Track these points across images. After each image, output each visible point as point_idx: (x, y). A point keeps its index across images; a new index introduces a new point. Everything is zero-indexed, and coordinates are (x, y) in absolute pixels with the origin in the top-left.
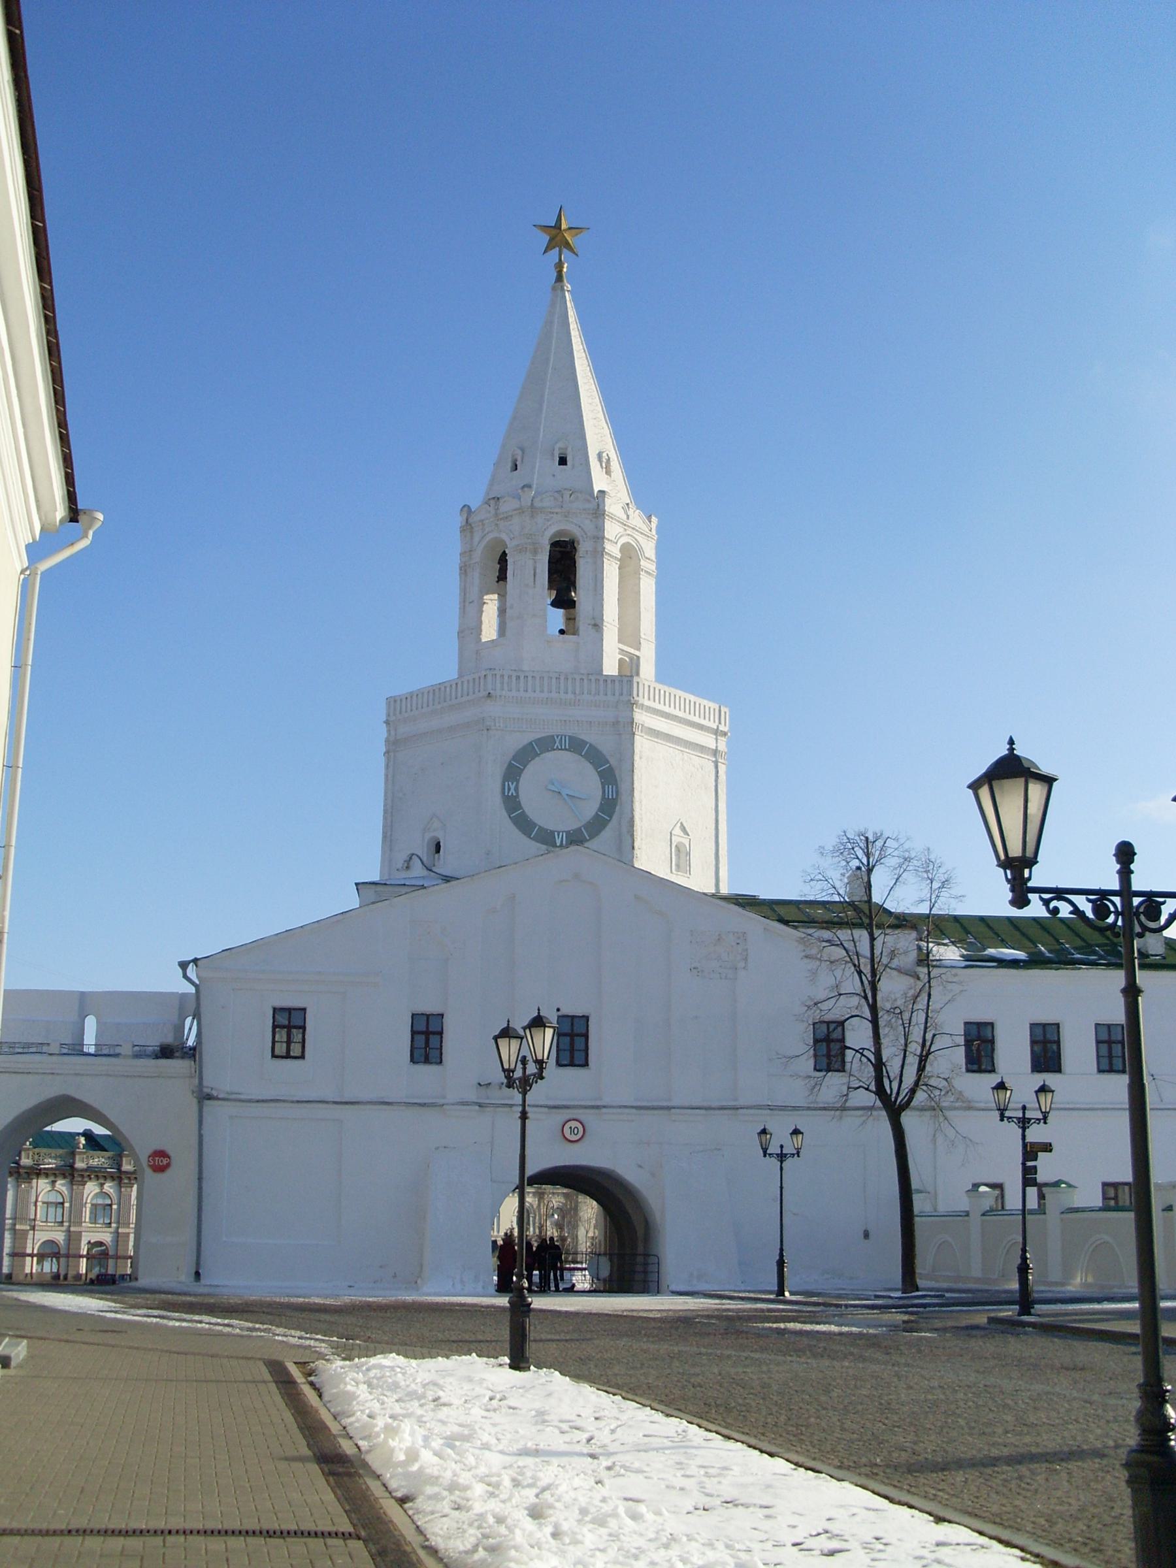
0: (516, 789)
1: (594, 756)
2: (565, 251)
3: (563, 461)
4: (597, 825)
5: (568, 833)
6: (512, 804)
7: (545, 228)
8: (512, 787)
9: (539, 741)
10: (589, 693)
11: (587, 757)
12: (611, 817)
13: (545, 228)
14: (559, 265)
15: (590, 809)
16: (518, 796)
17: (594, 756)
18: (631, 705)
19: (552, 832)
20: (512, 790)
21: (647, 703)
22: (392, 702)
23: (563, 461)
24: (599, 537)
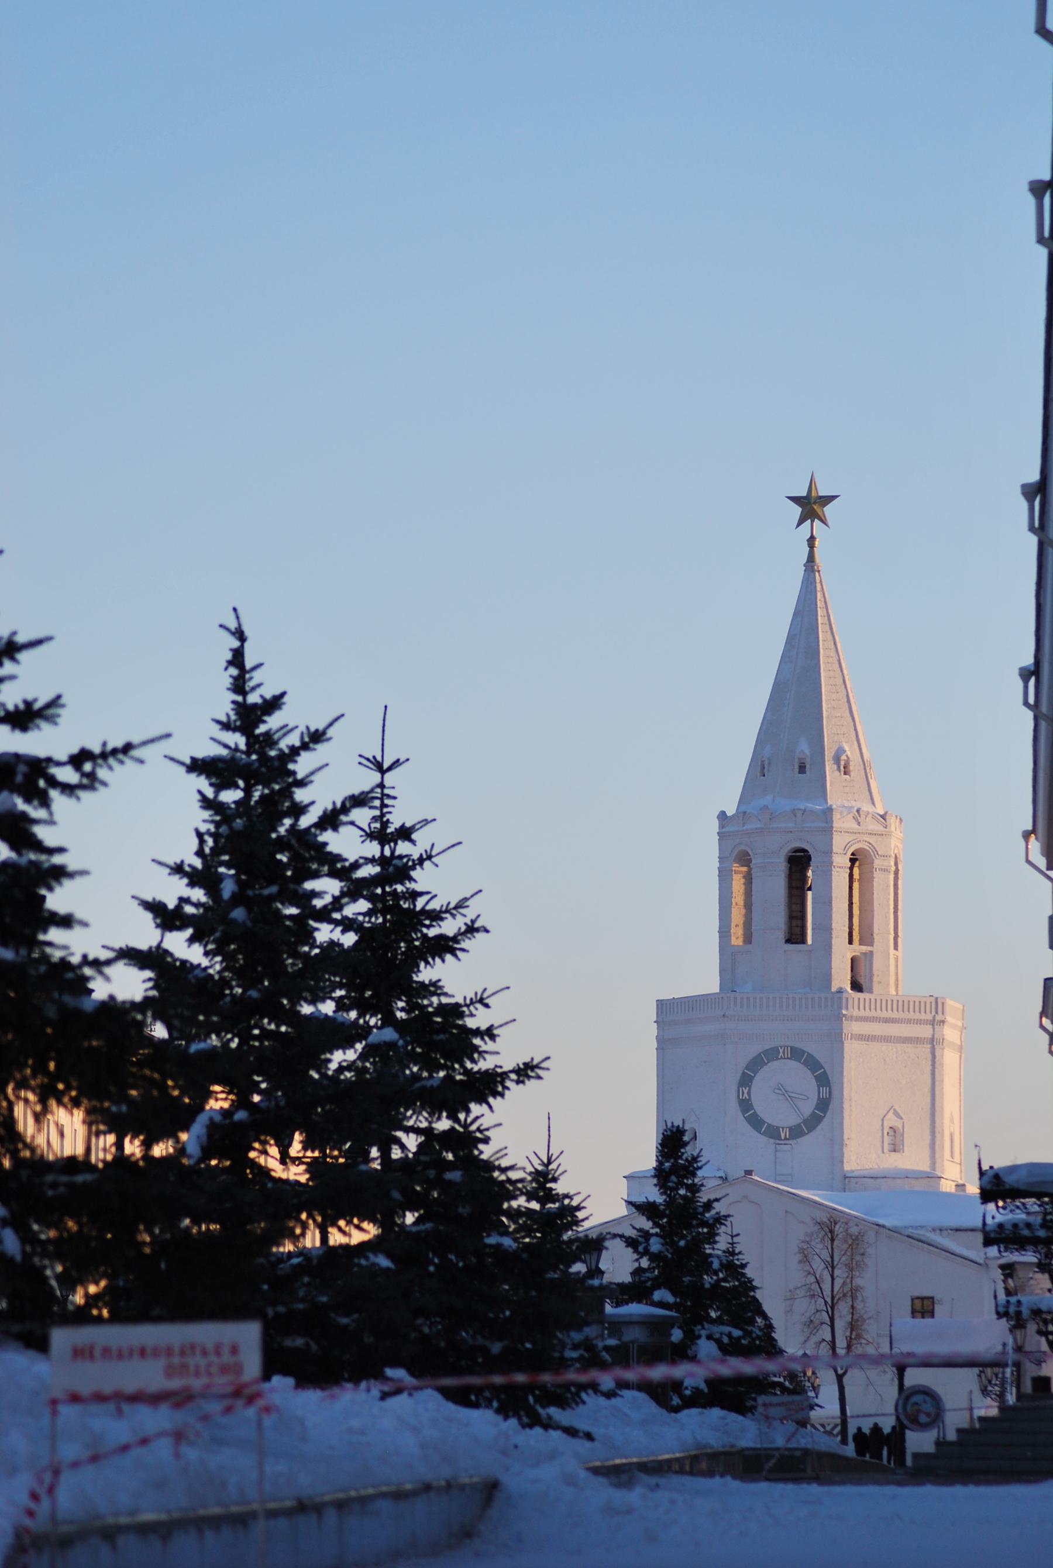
0: (749, 1093)
1: (812, 1064)
2: (817, 522)
3: (802, 769)
4: (813, 1122)
5: (790, 1129)
6: (745, 1105)
7: (795, 500)
8: (746, 1091)
9: (766, 1052)
10: (820, 998)
11: (805, 1064)
12: (825, 1113)
13: (795, 500)
14: (811, 540)
15: (808, 1108)
16: (750, 1099)
17: (812, 1064)
18: (839, 1018)
19: (778, 1128)
20: (746, 1095)
21: (856, 1013)
22: (660, 1003)
23: (802, 769)
24: (829, 852)
